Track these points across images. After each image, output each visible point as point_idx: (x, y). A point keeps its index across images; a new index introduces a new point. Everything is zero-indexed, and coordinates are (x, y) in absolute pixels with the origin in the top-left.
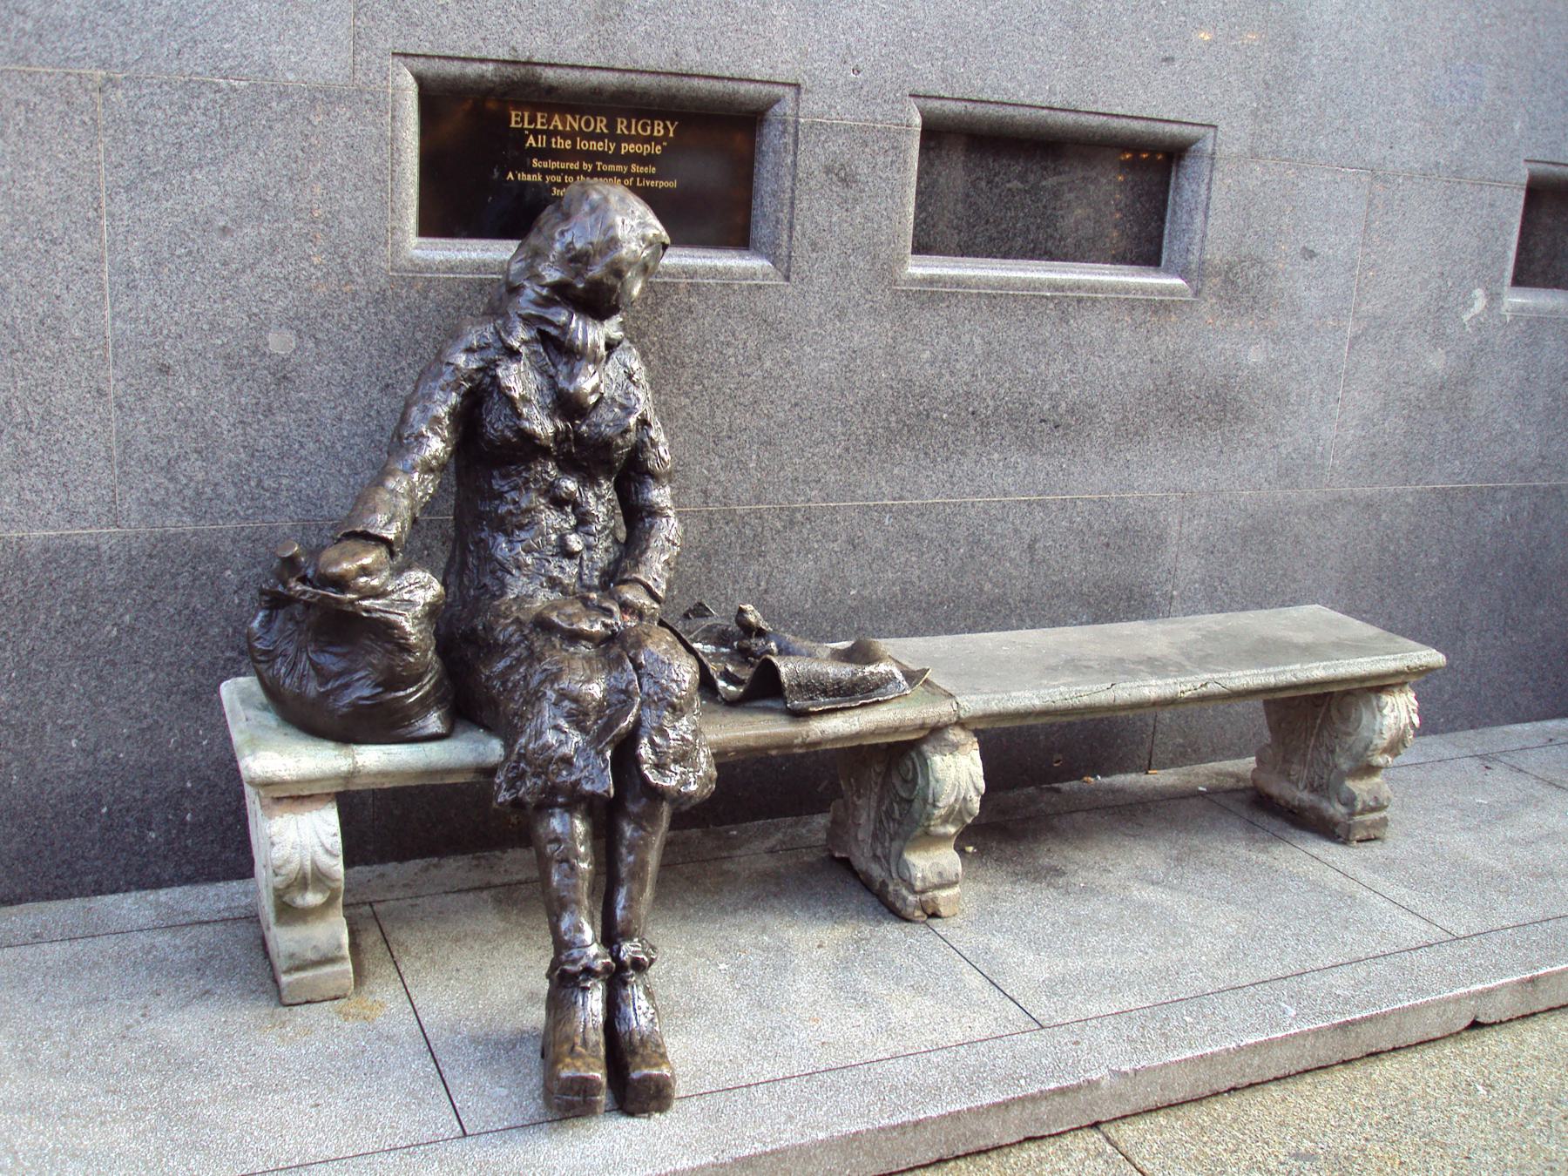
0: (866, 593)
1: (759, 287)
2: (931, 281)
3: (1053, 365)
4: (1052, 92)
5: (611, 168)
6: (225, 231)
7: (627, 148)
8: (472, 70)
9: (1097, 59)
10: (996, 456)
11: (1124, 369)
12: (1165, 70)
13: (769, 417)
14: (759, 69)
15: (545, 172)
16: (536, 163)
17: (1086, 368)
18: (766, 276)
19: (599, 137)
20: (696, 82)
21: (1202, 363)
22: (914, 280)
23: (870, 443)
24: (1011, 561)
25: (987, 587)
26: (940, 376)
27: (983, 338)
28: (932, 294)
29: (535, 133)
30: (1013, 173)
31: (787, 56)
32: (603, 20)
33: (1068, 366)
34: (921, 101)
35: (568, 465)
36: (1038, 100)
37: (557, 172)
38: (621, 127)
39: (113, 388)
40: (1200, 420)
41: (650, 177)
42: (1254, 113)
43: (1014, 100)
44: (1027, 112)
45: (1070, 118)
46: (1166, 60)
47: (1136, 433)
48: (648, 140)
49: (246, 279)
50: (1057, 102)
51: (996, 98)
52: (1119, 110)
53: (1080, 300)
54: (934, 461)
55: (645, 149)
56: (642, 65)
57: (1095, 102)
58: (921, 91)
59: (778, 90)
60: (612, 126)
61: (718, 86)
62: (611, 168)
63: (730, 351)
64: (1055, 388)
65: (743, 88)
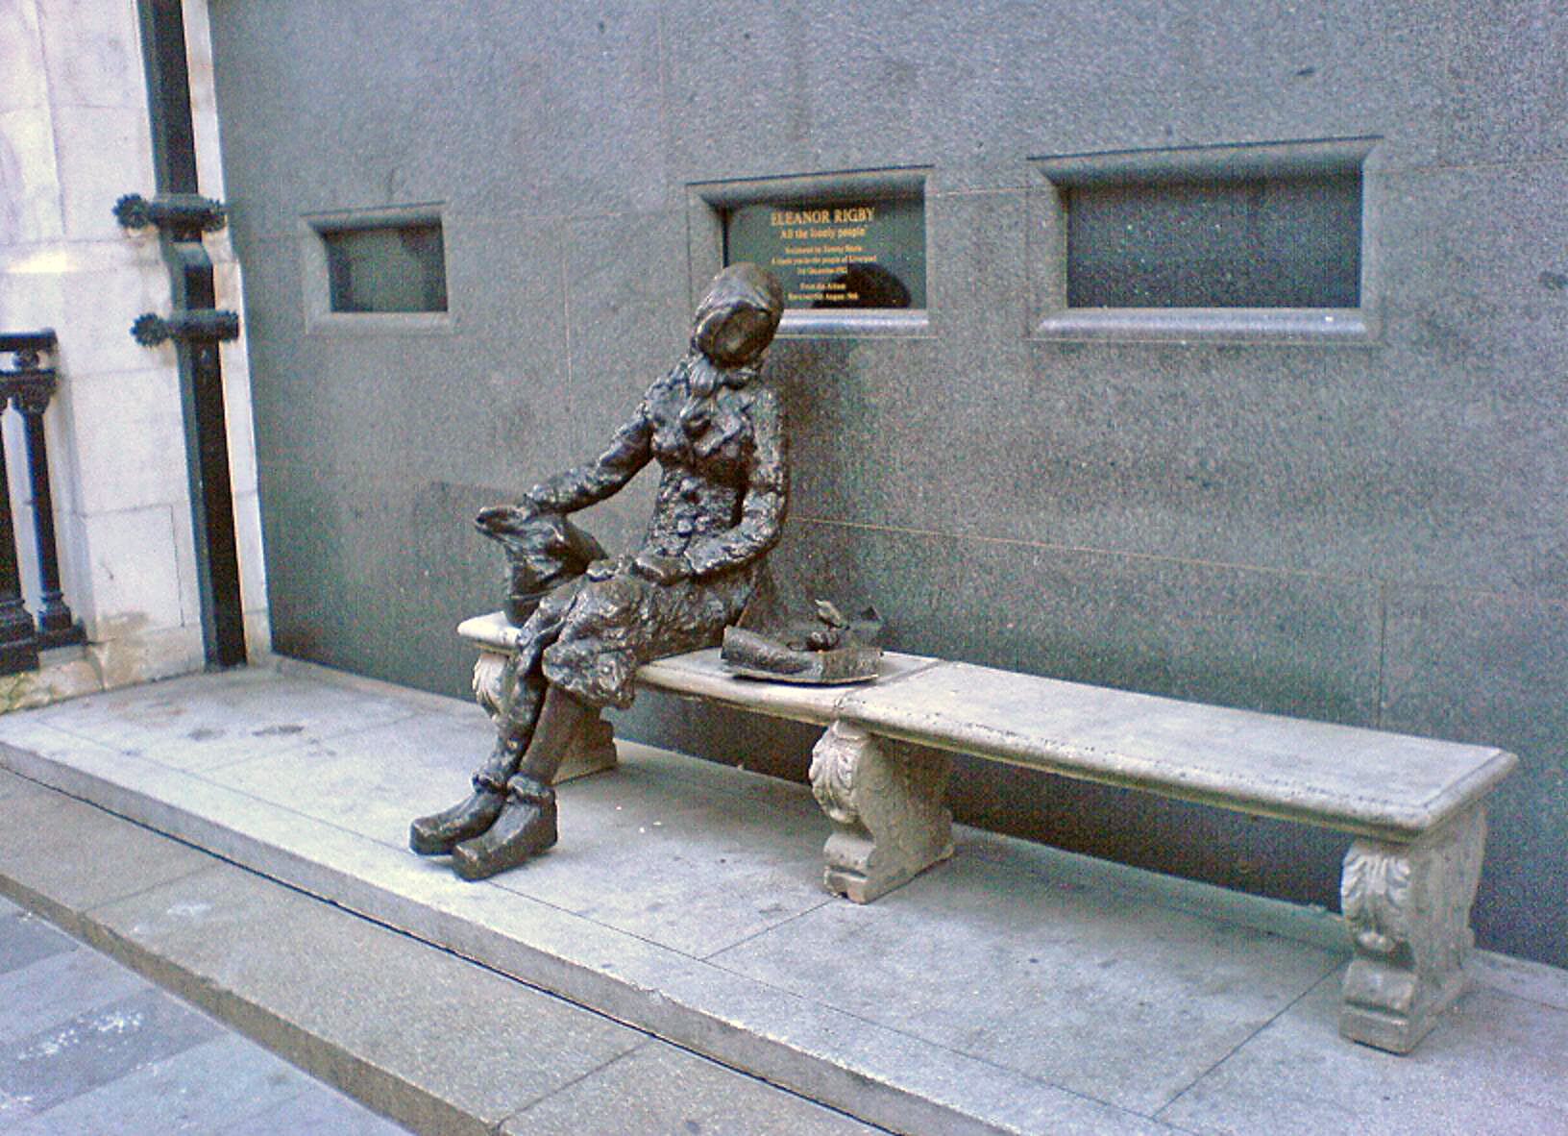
0: (1022, 628)
1: (916, 342)
2: (1064, 333)
3: (1196, 419)
4: (1169, 132)
5: (833, 250)
6: (615, 309)
7: (843, 233)
8: (729, 187)
9: (1215, 88)
10: (1140, 510)
11: (1283, 425)
12: (1304, 84)
13: (931, 454)
14: (902, 157)
15: (793, 257)
16: (788, 251)
17: (1235, 424)
18: (922, 331)
19: (824, 226)
20: (862, 176)
21: (1393, 423)
22: (1047, 333)
23: (1016, 486)
24: (1167, 625)
25: (1143, 648)
26: (1078, 426)
27: (1115, 387)
28: (1068, 346)
29: (786, 228)
30: (1120, 222)
31: (923, 143)
32: (798, 138)
33: (1214, 419)
34: (1039, 163)
35: (693, 470)
36: (1154, 142)
37: (801, 256)
38: (838, 218)
39: (573, 407)
40: (1398, 492)
41: (857, 254)
42: (1438, 113)
43: (1128, 146)
44: (1147, 157)
45: (1194, 158)
46: (1302, 73)
47: (1308, 500)
48: (855, 225)
49: (625, 339)
50: (1175, 141)
51: (1111, 147)
52: (1250, 138)
53: (1221, 349)
54: (1077, 509)
55: (854, 233)
56: (824, 168)
57: (1219, 134)
58: (1036, 153)
59: (921, 172)
60: (832, 217)
61: (877, 176)
62: (833, 250)
63: (897, 396)
64: (1201, 444)
65: (896, 175)
